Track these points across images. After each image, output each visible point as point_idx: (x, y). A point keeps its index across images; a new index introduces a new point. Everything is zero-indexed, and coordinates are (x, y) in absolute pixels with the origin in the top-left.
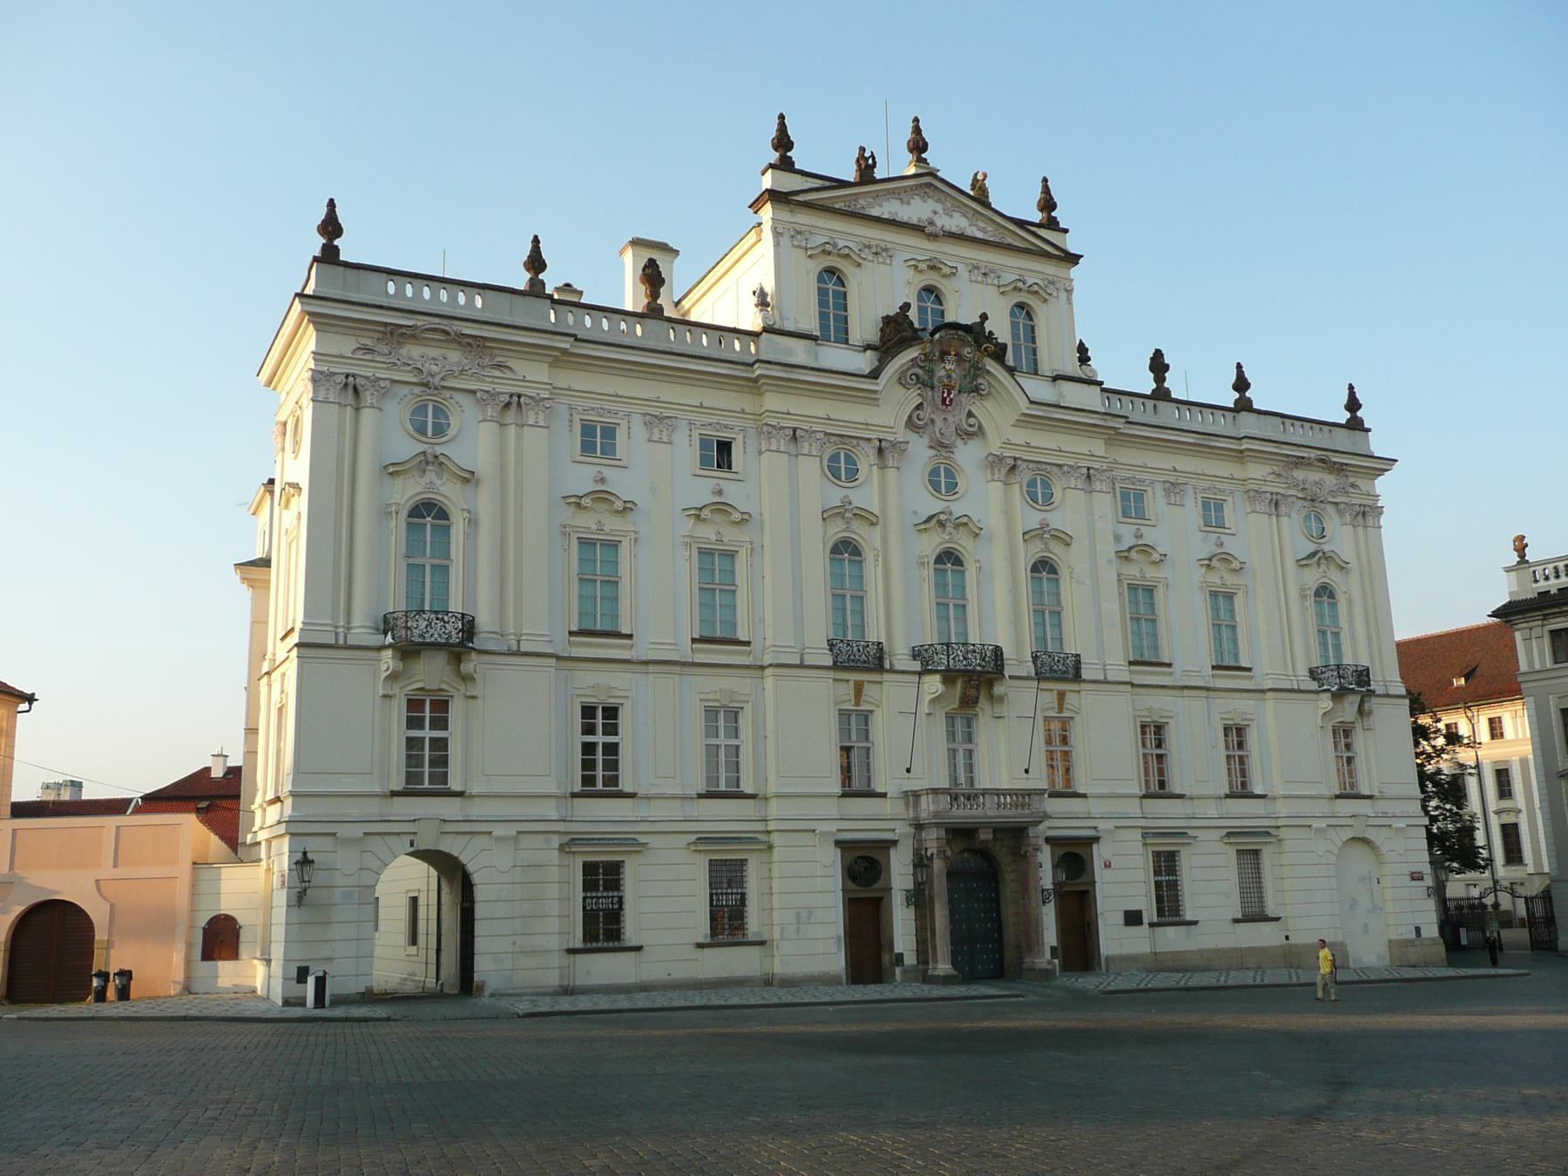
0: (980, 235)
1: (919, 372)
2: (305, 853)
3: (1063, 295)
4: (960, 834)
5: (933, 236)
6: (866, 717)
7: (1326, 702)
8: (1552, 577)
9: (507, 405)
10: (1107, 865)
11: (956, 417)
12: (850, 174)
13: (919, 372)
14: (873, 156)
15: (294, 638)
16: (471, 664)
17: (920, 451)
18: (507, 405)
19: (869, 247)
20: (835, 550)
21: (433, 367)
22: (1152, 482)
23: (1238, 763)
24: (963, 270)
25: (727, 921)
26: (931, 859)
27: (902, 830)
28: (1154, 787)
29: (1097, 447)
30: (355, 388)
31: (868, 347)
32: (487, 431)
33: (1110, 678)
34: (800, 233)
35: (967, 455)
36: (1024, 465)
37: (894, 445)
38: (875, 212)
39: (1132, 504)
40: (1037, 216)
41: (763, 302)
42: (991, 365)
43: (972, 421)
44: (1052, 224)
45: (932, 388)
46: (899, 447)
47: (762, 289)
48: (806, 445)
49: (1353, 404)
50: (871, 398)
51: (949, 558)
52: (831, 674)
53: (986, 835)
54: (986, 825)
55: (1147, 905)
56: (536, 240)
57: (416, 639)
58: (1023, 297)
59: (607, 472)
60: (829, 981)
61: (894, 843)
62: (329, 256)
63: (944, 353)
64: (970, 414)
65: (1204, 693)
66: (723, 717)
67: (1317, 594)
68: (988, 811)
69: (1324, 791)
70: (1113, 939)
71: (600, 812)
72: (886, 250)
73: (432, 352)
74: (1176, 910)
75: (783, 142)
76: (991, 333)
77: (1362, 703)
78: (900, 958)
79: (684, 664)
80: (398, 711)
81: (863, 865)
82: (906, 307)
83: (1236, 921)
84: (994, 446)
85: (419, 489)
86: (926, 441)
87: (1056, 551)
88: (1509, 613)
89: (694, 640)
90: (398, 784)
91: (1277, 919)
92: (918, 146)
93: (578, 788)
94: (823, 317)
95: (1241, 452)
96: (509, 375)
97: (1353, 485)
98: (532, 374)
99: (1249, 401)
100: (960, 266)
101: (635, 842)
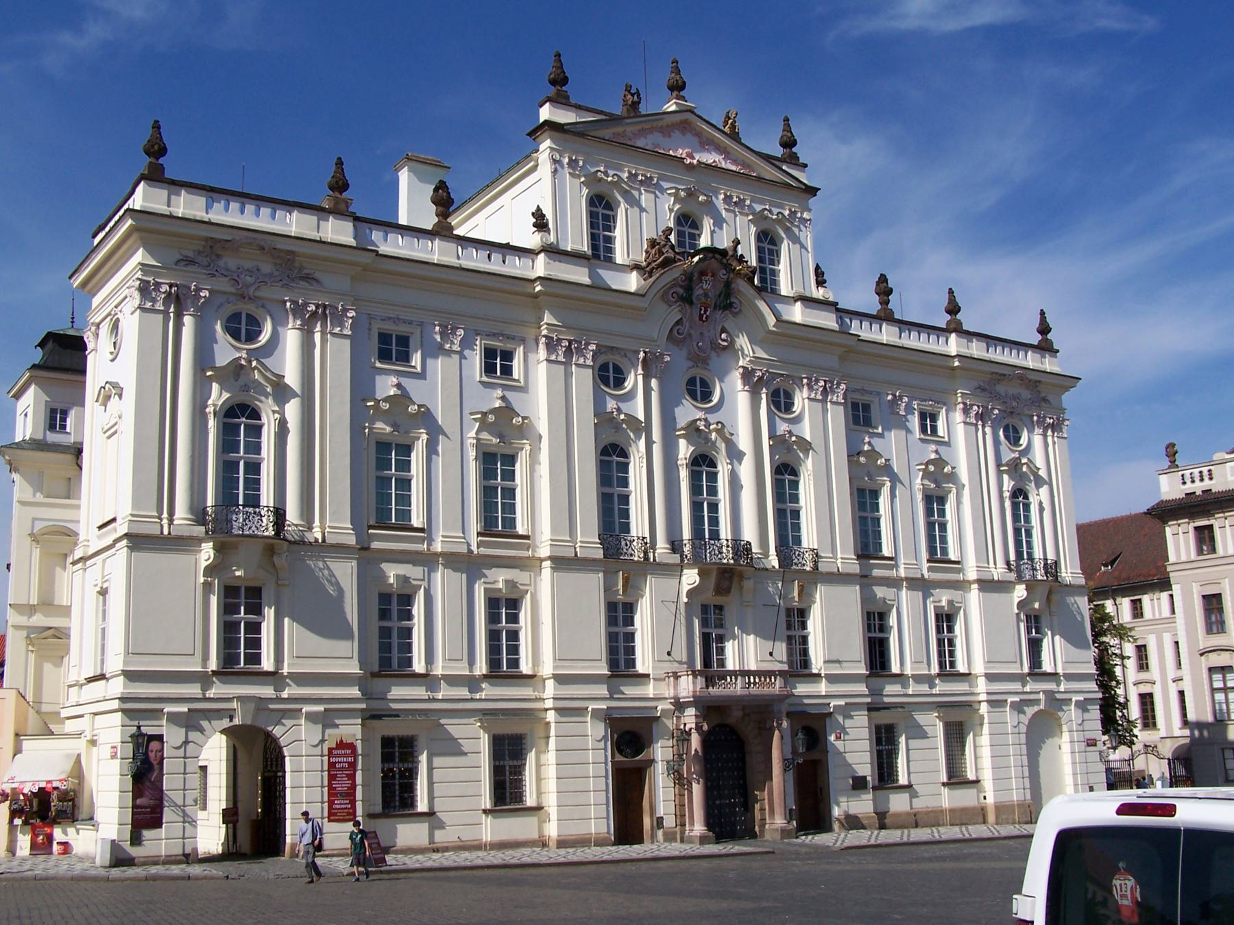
0: (734, 168)
2: (139, 727)
8: (1197, 479)
12: (618, 110)
13: (681, 291)
15: (122, 528)
21: (248, 279)
23: (946, 648)
25: (507, 792)
26: (689, 733)
30: (177, 296)
32: (291, 338)
40: (778, 152)
41: (540, 223)
42: (741, 285)
44: (793, 160)
45: (691, 303)
47: (539, 209)
49: (1044, 329)
51: (703, 463)
57: (235, 532)
60: (600, 842)
63: (703, 273)
66: (504, 607)
68: (737, 687)
78: (660, 820)
81: (630, 737)
86: (684, 353)
88: (1166, 512)
93: (376, 668)
94: (593, 238)
99: (960, 323)
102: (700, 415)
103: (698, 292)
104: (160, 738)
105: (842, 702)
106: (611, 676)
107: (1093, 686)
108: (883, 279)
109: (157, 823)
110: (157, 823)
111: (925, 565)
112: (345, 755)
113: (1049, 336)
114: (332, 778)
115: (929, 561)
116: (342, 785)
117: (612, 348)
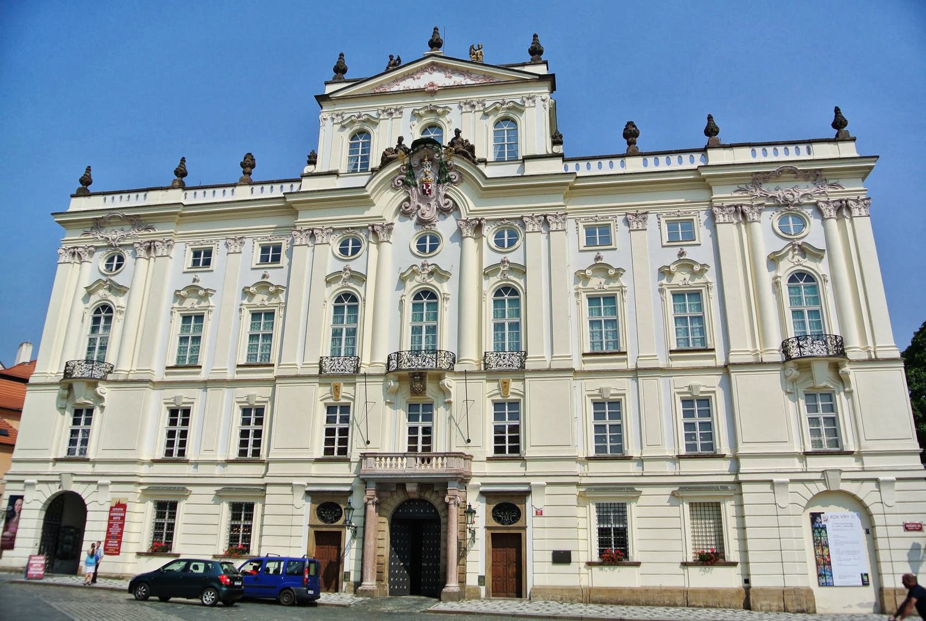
4: (385, 487)
5: (433, 93)
6: (346, 408)
9: (149, 249)
14: (399, 59)
16: (102, 388)
18: (149, 249)
20: (339, 299)
24: (454, 107)
30: (79, 254)
31: (373, 170)
39: (599, 235)
42: (457, 162)
43: (447, 200)
45: (416, 186)
48: (320, 238)
52: (318, 381)
53: (410, 488)
54: (411, 481)
55: (587, 546)
59: (200, 276)
64: (446, 196)
67: (792, 279)
70: (539, 572)
72: (396, 110)
76: (467, 141)
77: (836, 367)
81: (328, 506)
82: (400, 139)
85: (99, 298)
90: (63, 454)
96: (152, 232)
97: (832, 185)
102: (419, 262)
104: (21, 497)
105: (542, 481)
108: (630, 124)
112: (120, 512)
113: (845, 129)
114: (110, 526)
116: (115, 531)
117: (348, 228)
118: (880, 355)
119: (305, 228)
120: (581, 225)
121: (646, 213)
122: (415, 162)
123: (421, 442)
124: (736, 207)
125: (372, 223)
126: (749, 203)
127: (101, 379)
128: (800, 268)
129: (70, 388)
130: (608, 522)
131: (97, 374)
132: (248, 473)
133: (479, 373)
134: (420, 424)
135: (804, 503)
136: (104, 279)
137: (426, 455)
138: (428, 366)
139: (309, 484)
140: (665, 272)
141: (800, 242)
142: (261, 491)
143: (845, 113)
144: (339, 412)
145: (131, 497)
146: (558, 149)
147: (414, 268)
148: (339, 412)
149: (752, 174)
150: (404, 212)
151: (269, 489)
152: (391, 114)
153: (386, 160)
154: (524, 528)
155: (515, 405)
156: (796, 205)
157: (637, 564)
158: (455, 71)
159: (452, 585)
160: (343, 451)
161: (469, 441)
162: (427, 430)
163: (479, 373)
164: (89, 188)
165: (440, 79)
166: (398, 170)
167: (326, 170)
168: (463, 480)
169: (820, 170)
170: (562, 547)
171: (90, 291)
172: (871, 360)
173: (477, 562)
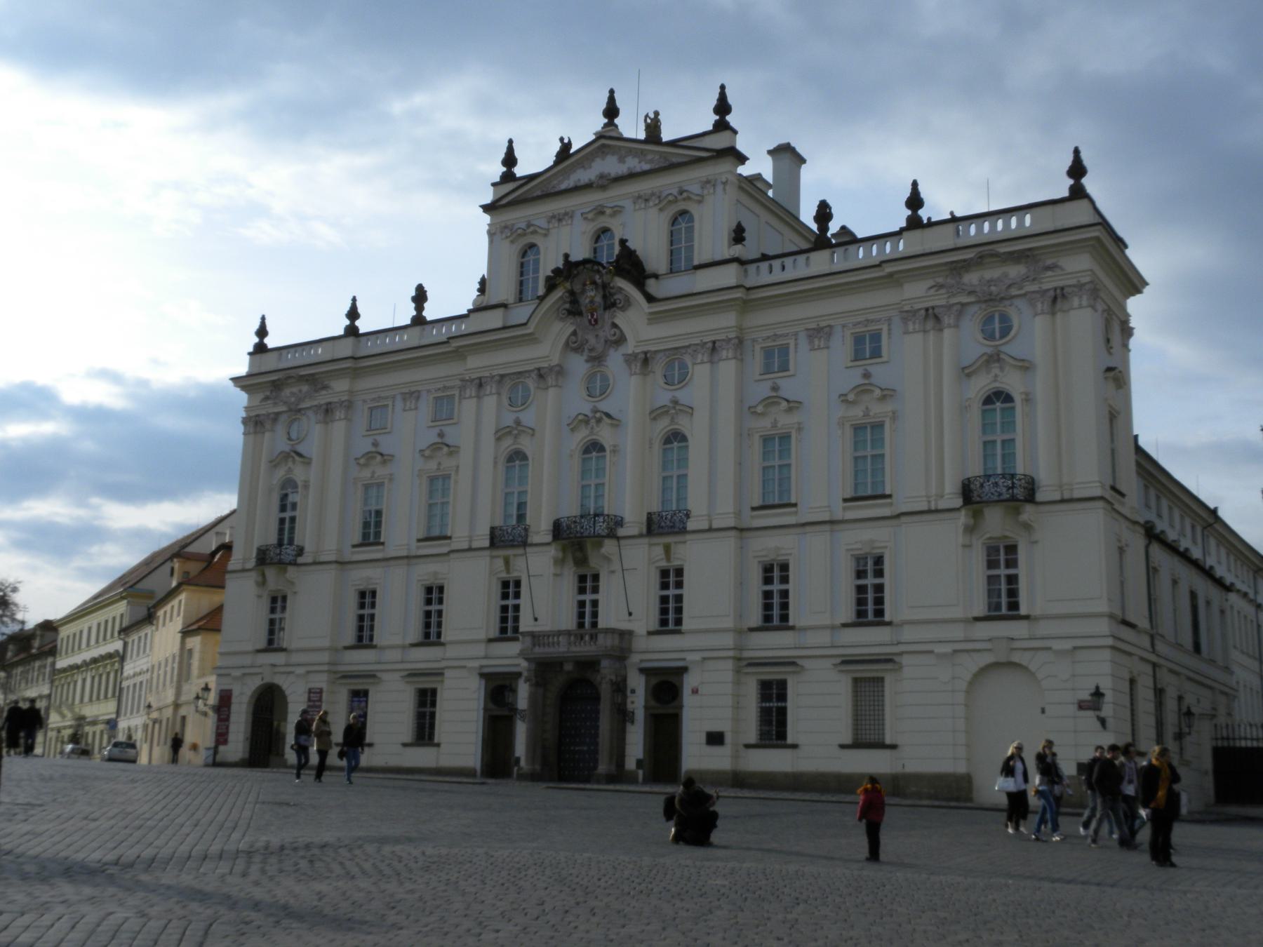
0: (646, 167)
1: (567, 306)
3: (720, 188)
5: (603, 187)
6: (518, 583)
7: (963, 518)
9: (327, 411)
10: (695, 691)
11: (606, 332)
17: (578, 365)
19: (553, 217)
20: (510, 459)
22: (796, 334)
24: (628, 204)
27: (524, 664)
28: (776, 621)
29: (726, 321)
31: (538, 297)
33: (715, 526)
34: (506, 227)
35: (615, 361)
36: (661, 355)
37: (551, 369)
38: (563, 186)
42: (621, 283)
44: (722, 126)
45: (580, 314)
46: (560, 371)
49: (1077, 170)
50: (531, 339)
52: (487, 553)
53: (568, 667)
56: (354, 300)
58: (682, 206)
61: (519, 675)
62: (260, 349)
64: (615, 326)
65: (827, 527)
67: (988, 400)
69: (958, 613)
71: (361, 659)
72: (566, 214)
73: (295, 390)
74: (782, 735)
75: (510, 160)
78: (518, 760)
79: (407, 557)
80: (265, 604)
81: (498, 689)
82: (566, 256)
83: (843, 747)
84: (630, 347)
86: (585, 357)
87: (683, 424)
89: (419, 540)
90: (262, 644)
91: (893, 747)
92: (611, 111)
95: (891, 275)
97: (1049, 268)
98: (340, 386)
100: (620, 203)
101: (374, 676)
103: (584, 301)
105: (696, 657)
106: (490, 641)
107: (1103, 627)
109: (225, 742)
110: (225, 742)
111: (841, 504)
113: (1084, 181)
115: (845, 500)
118: (1076, 495)
119: (474, 376)
120: (757, 348)
121: (830, 326)
122: (577, 288)
123: (587, 614)
124: (927, 310)
125: (537, 366)
126: (943, 302)
127: (290, 564)
128: (997, 385)
129: (263, 575)
130: (770, 700)
131: (288, 559)
132: (425, 657)
133: (641, 536)
134: (588, 597)
135: (968, 677)
136: (287, 449)
137: (593, 631)
138: (586, 534)
139: (482, 667)
140: (843, 398)
141: (1003, 349)
142: (439, 674)
143: (1085, 157)
144: (510, 588)
145: (324, 686)
146: (737, 250)
147: (580, 417)
148: (510, 588)
149: (946, 264)
150: (574, 345)
151: (448, 673)
152: (560, 220)
153: (551, 285)
154: (681, 707)
155: (679, 572)
156: (1002, 299)
157: (795, 746)
158: (631, 152)
159: (603, 768)
160: (516, 629)
161: (630, 614)
162: (595, 603)
163: (641, 536)
164: (266, 341)
165: (611, 165)
166: (561, 298)
167: (494, 302)
168: (621, 655)
169: (1030, 249)
170: (715, 727)
171: (274, 464)
172: (1063, 501)
173: (636, 745)
